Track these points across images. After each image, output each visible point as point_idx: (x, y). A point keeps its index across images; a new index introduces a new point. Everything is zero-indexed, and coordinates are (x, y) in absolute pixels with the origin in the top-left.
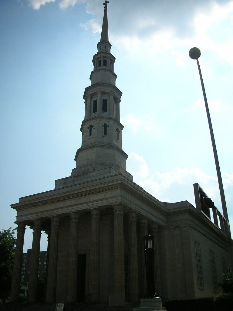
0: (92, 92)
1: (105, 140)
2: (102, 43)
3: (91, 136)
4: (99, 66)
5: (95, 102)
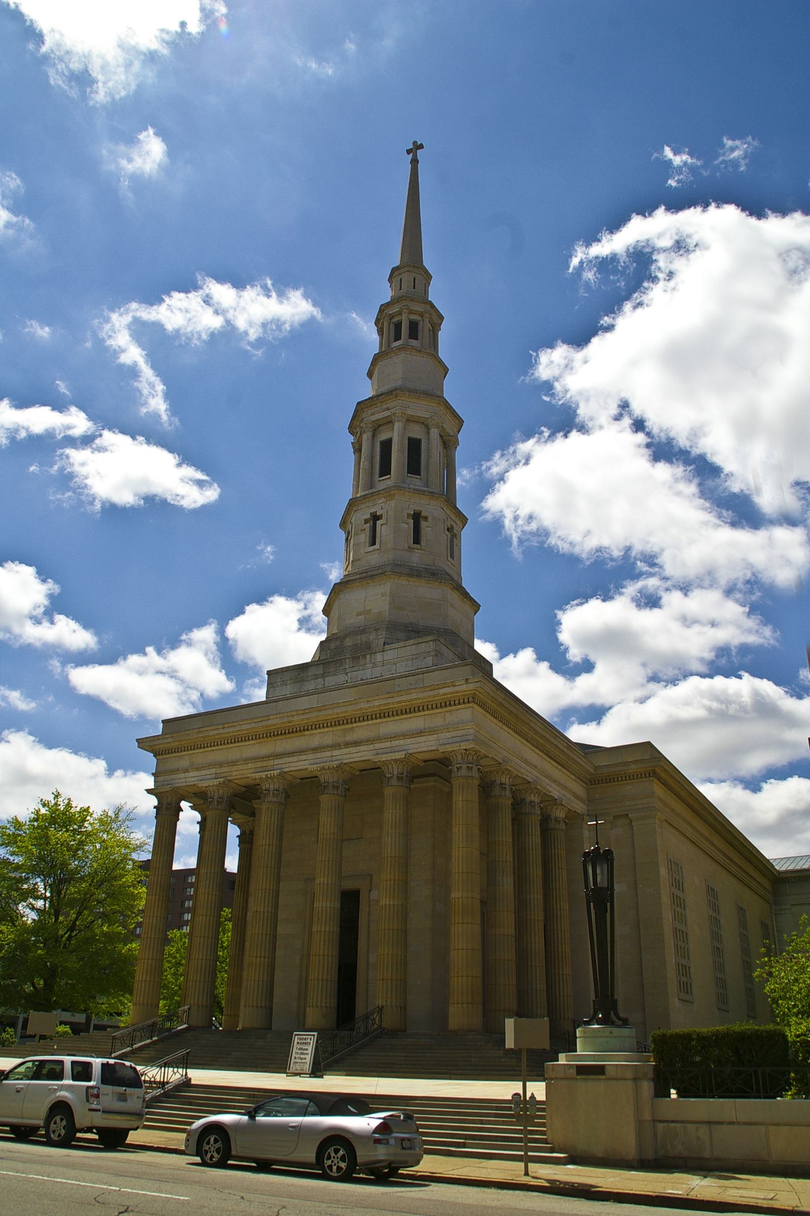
1: (416, 558)
2: (406, 269)
3: (374, 543)
4: (398, 337)
5: (387, 446)
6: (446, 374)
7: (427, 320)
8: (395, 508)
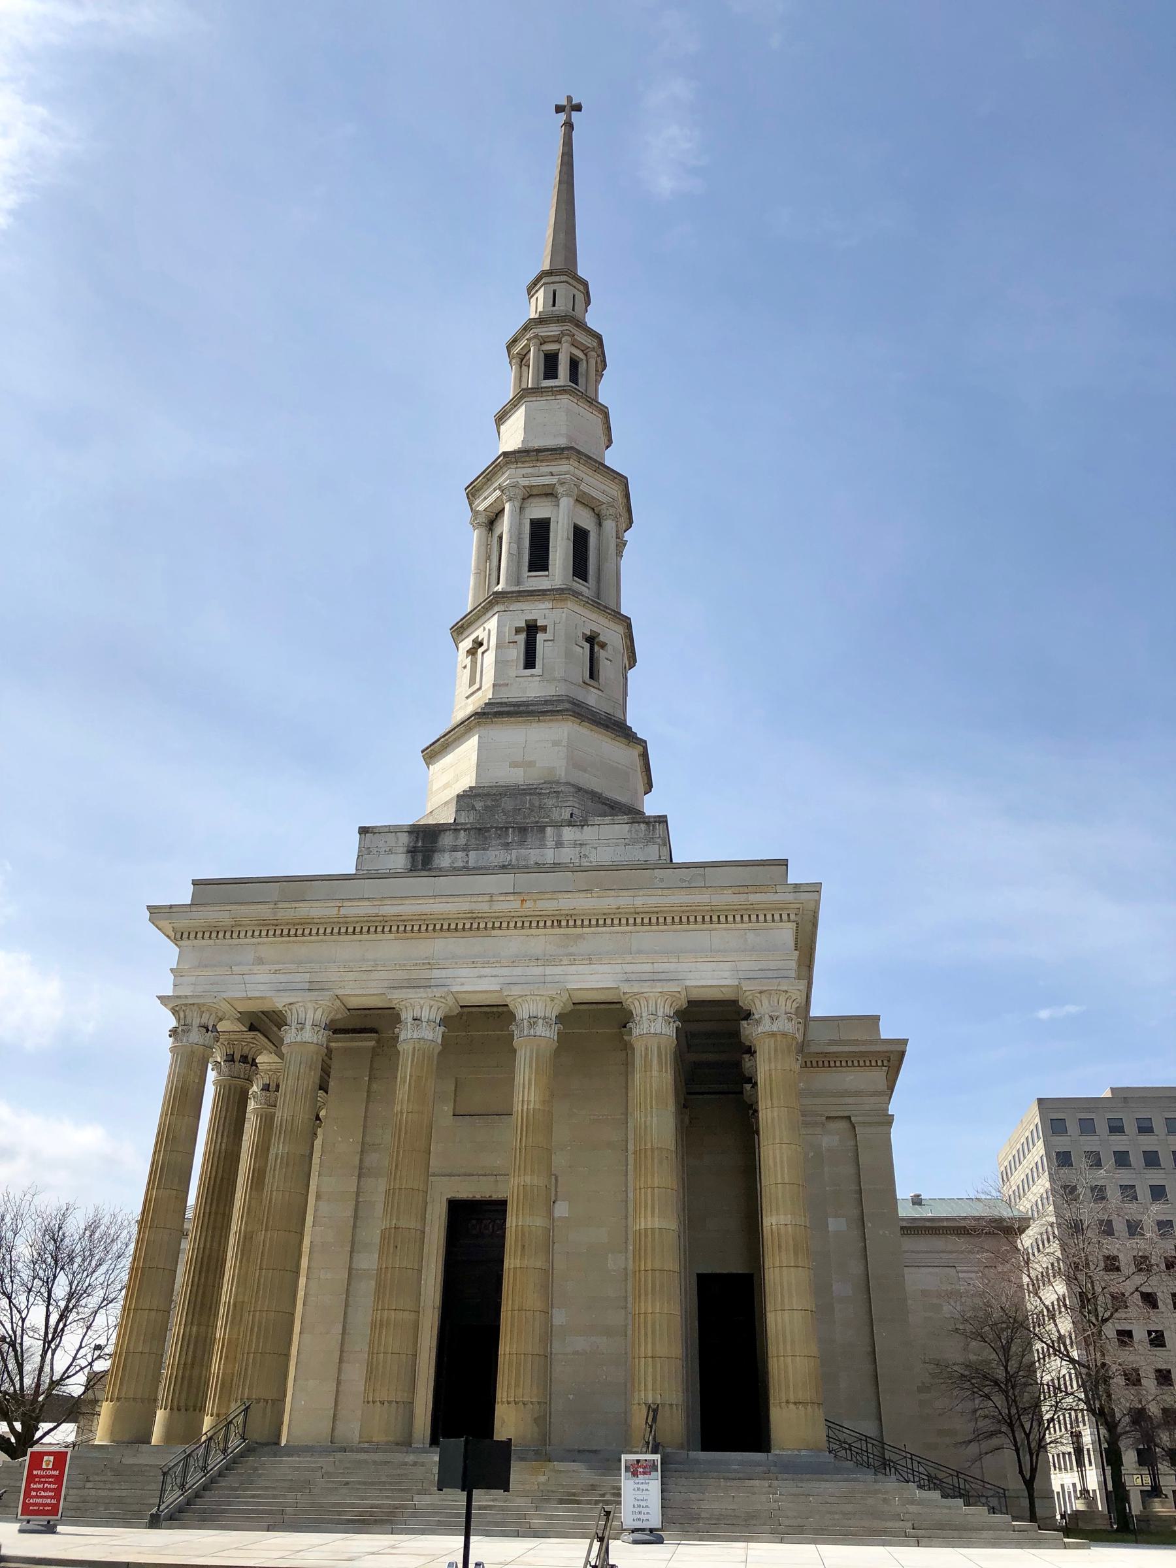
0: (535, 481)
1: (592, 698)
2: (564, 278)
6: (608, 447)
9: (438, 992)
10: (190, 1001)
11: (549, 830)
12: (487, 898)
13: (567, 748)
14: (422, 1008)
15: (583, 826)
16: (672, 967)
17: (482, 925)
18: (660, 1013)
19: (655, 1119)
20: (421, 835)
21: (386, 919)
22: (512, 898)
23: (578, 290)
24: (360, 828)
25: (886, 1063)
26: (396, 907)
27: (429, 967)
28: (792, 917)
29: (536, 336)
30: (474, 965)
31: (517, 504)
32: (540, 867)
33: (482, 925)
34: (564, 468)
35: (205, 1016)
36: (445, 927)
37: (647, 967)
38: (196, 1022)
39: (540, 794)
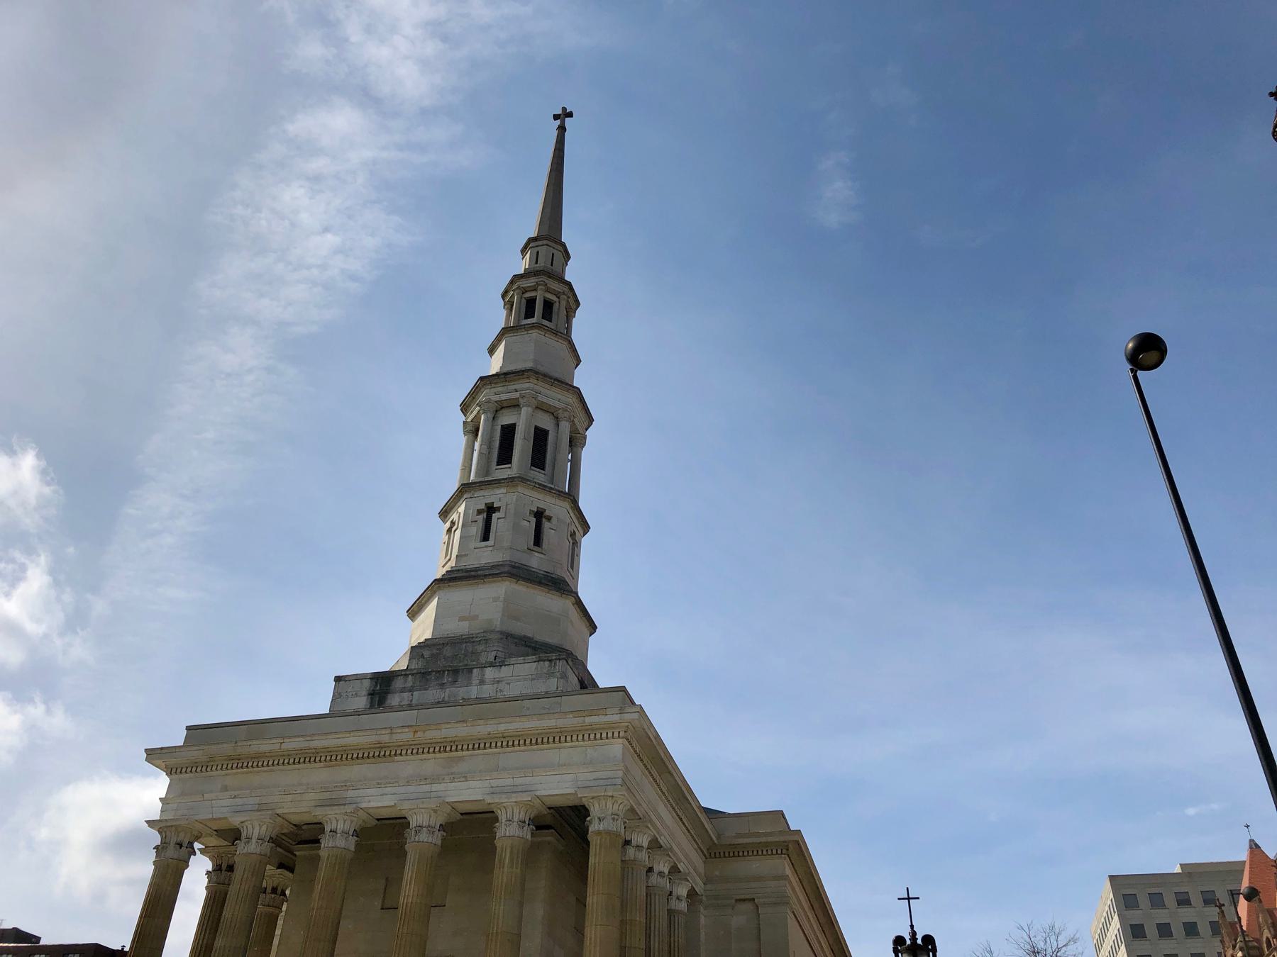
0: (504, 397)
1: (536, 561)
2: (545, 242)
5: (508, 433)
6: (577, 365)
7: (564, 303)
8: (516, 501)
9: (349, 809)
10: (169, 824)
11: (475, 670)
12: (388, 731)
13: (504, 604)
14: (337, 821)
15: (501, 666)
16: (528, 780)
17: (388, 753)
18: (516, 819)
19: (502, 907)
20: (380, 681)
21: (318, 751)
22: (407, 730)
23: (557, 250)
24: (336, 677)
25: (784, 851)
26: (324, 741)
27: (344, 788)
28: (622, 734)
29: (519, 288)
30: (379, 786)
31: (491, 415)
32: (466, 702)
33: (388, 753)
34: (526, 385)
35: (182, 835)
36: (360, 756)
37: (509, 782)
38: (173, 841)
39: (473, 642)
